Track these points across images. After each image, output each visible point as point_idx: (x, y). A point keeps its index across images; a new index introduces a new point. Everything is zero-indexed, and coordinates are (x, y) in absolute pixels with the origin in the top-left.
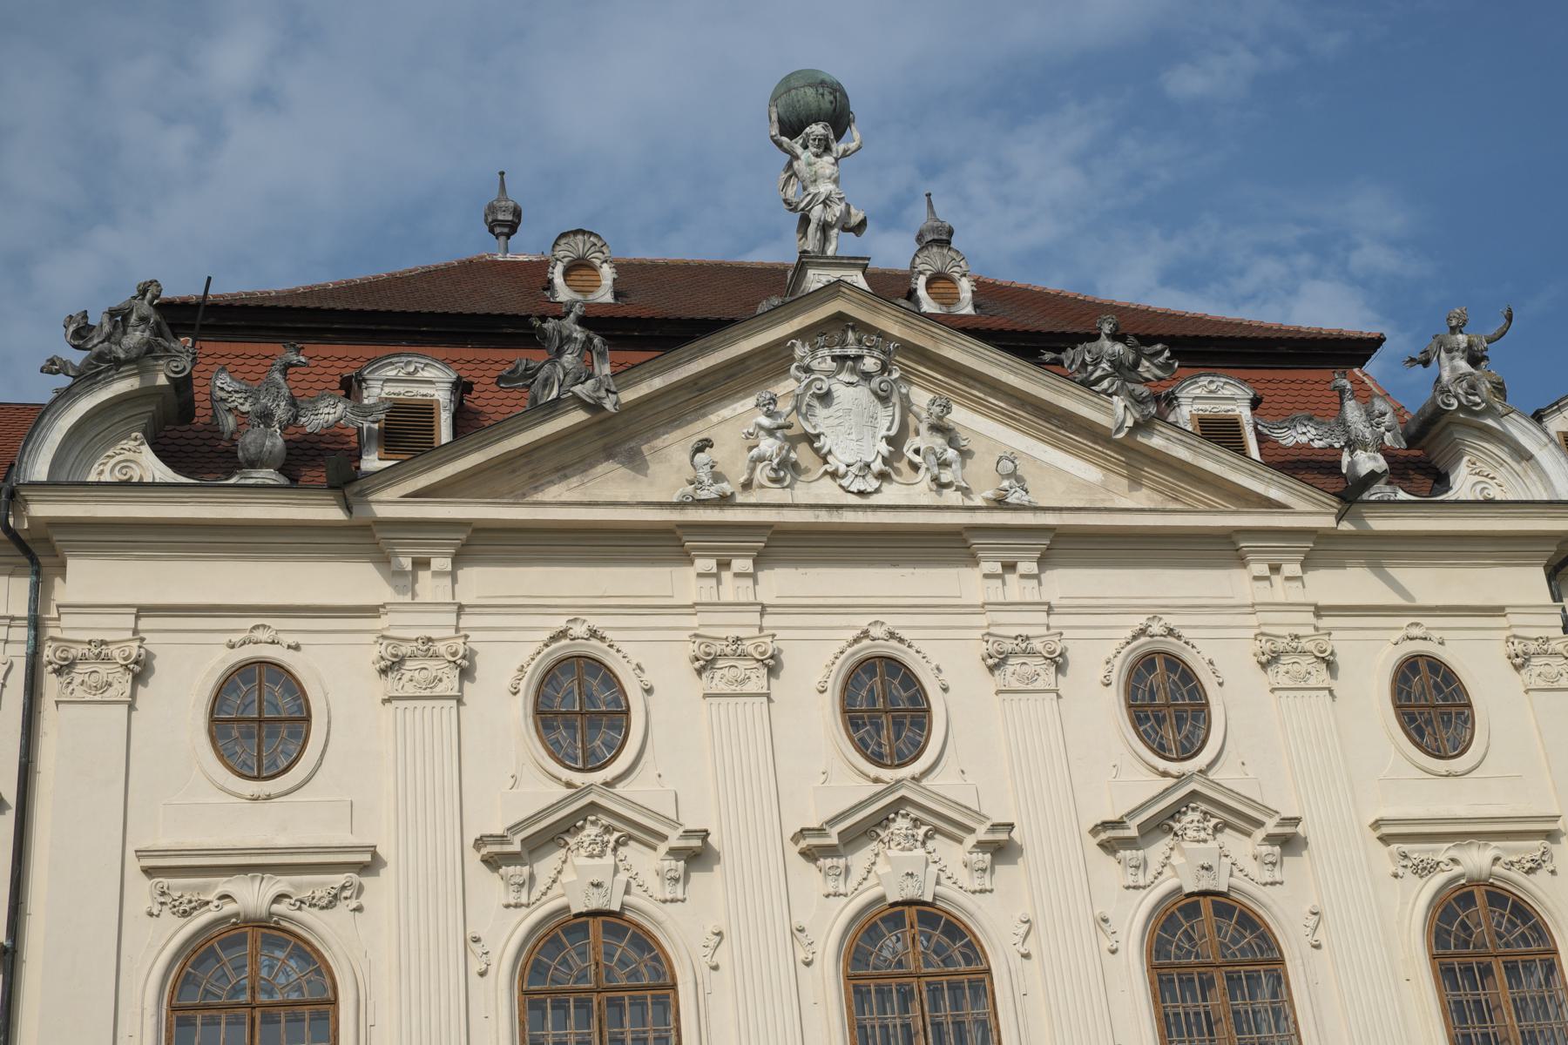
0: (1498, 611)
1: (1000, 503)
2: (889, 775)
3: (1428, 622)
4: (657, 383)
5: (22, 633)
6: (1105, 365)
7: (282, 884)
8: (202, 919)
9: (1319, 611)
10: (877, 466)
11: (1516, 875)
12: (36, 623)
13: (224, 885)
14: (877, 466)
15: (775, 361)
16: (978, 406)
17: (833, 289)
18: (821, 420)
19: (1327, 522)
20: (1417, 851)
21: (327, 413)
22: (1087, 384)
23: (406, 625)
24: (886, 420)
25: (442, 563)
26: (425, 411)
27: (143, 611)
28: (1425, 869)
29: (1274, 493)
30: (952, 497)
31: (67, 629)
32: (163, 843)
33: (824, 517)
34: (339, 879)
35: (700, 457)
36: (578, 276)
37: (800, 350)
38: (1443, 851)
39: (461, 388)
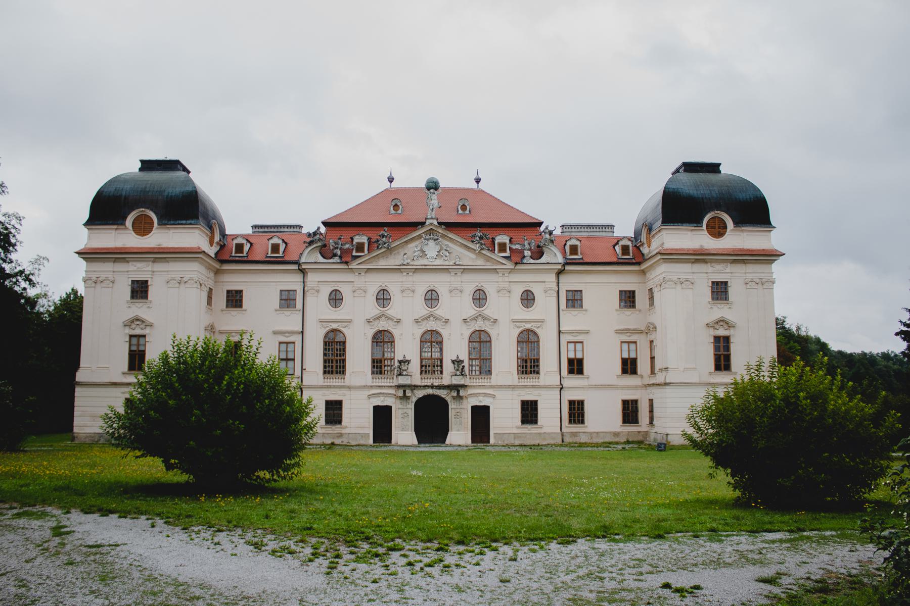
0: (544, 282)
1: (455, 264)
2: (430, 309)
3: (530, 284)
4: (399, 243)
5: (302, 284)
6: (478, 238)
7: (339, 324)
8: (328, 329)
9: (510, 282)
10: (435, 257)
11: (535, 329)
12: (304, 282)
13: (331, 324)
14: (435, 257)
15: (420, 237)
16: (455, 244)
17: (431, 224)
18: (425, 249)
19: (513, 267)
20: (518, 324)
21: (347, 246)
22: (473, 242)
23: (357, 285)
24: (438, 248)
25: (363, 274)
26: (363, 244)
27: (319, 282)
28: (519, 327)
29: (504, 262)
30: (447, 263)
31: (309, 285)
32: (322, 318)
33: (424, 267)
34: (347, 324)
35: (405, 256)
36: (396, 208)
37: (424, 236)
38: (522, 324)
39: (369, 239)
